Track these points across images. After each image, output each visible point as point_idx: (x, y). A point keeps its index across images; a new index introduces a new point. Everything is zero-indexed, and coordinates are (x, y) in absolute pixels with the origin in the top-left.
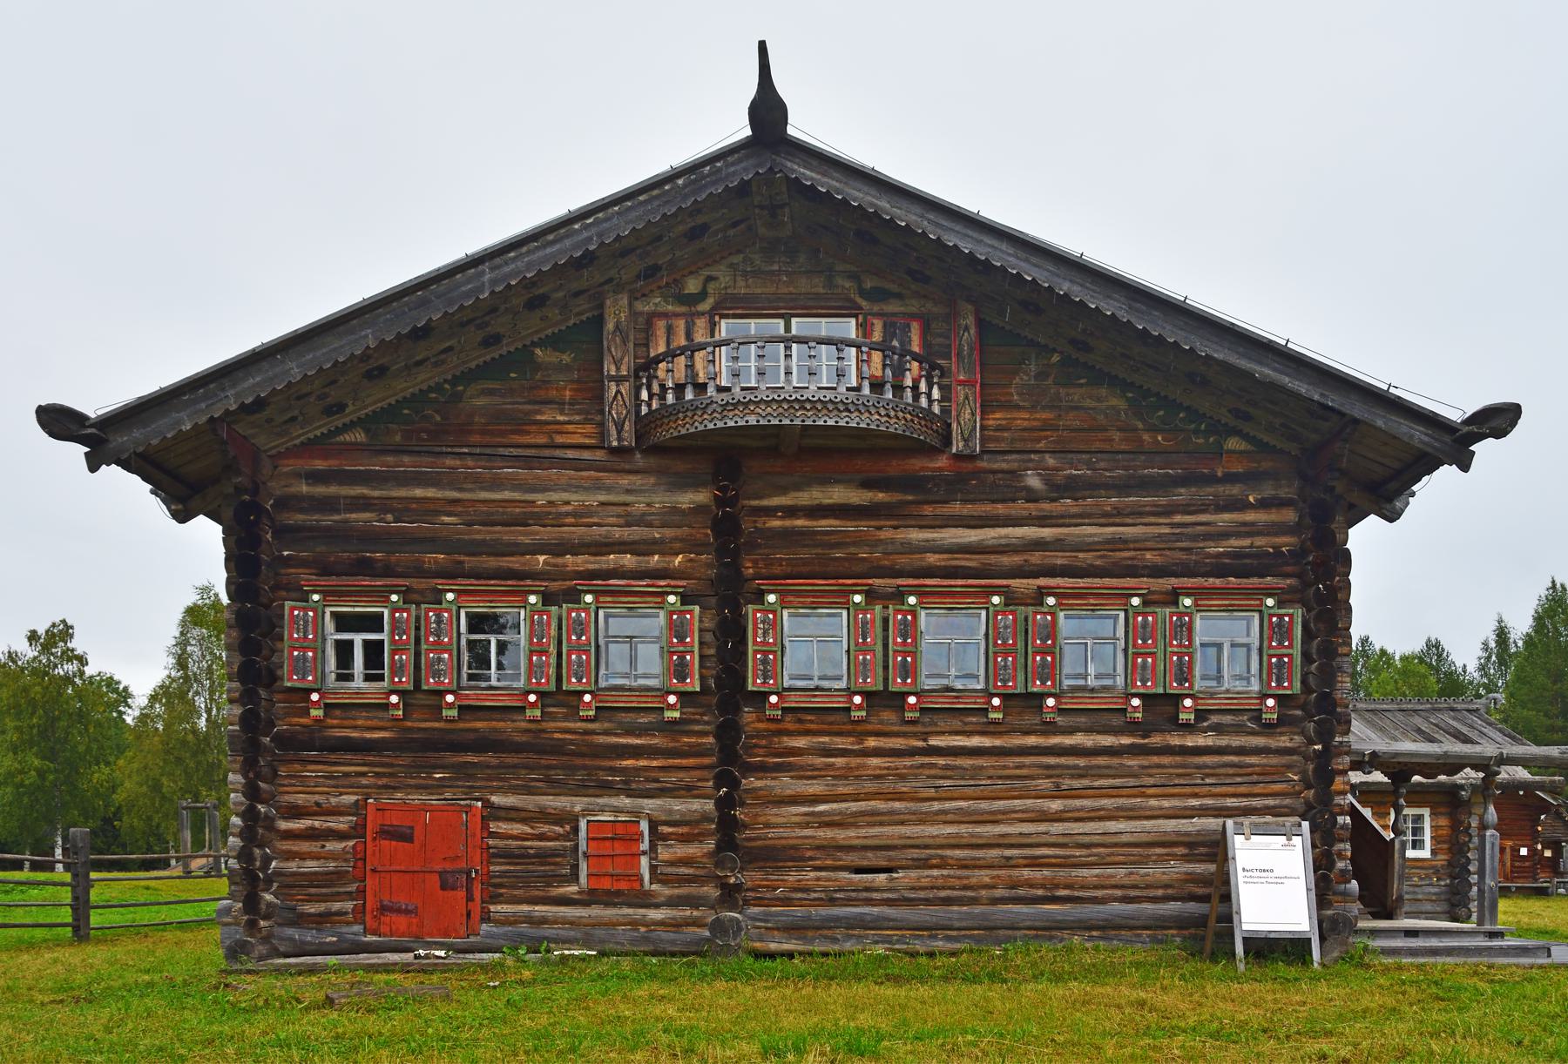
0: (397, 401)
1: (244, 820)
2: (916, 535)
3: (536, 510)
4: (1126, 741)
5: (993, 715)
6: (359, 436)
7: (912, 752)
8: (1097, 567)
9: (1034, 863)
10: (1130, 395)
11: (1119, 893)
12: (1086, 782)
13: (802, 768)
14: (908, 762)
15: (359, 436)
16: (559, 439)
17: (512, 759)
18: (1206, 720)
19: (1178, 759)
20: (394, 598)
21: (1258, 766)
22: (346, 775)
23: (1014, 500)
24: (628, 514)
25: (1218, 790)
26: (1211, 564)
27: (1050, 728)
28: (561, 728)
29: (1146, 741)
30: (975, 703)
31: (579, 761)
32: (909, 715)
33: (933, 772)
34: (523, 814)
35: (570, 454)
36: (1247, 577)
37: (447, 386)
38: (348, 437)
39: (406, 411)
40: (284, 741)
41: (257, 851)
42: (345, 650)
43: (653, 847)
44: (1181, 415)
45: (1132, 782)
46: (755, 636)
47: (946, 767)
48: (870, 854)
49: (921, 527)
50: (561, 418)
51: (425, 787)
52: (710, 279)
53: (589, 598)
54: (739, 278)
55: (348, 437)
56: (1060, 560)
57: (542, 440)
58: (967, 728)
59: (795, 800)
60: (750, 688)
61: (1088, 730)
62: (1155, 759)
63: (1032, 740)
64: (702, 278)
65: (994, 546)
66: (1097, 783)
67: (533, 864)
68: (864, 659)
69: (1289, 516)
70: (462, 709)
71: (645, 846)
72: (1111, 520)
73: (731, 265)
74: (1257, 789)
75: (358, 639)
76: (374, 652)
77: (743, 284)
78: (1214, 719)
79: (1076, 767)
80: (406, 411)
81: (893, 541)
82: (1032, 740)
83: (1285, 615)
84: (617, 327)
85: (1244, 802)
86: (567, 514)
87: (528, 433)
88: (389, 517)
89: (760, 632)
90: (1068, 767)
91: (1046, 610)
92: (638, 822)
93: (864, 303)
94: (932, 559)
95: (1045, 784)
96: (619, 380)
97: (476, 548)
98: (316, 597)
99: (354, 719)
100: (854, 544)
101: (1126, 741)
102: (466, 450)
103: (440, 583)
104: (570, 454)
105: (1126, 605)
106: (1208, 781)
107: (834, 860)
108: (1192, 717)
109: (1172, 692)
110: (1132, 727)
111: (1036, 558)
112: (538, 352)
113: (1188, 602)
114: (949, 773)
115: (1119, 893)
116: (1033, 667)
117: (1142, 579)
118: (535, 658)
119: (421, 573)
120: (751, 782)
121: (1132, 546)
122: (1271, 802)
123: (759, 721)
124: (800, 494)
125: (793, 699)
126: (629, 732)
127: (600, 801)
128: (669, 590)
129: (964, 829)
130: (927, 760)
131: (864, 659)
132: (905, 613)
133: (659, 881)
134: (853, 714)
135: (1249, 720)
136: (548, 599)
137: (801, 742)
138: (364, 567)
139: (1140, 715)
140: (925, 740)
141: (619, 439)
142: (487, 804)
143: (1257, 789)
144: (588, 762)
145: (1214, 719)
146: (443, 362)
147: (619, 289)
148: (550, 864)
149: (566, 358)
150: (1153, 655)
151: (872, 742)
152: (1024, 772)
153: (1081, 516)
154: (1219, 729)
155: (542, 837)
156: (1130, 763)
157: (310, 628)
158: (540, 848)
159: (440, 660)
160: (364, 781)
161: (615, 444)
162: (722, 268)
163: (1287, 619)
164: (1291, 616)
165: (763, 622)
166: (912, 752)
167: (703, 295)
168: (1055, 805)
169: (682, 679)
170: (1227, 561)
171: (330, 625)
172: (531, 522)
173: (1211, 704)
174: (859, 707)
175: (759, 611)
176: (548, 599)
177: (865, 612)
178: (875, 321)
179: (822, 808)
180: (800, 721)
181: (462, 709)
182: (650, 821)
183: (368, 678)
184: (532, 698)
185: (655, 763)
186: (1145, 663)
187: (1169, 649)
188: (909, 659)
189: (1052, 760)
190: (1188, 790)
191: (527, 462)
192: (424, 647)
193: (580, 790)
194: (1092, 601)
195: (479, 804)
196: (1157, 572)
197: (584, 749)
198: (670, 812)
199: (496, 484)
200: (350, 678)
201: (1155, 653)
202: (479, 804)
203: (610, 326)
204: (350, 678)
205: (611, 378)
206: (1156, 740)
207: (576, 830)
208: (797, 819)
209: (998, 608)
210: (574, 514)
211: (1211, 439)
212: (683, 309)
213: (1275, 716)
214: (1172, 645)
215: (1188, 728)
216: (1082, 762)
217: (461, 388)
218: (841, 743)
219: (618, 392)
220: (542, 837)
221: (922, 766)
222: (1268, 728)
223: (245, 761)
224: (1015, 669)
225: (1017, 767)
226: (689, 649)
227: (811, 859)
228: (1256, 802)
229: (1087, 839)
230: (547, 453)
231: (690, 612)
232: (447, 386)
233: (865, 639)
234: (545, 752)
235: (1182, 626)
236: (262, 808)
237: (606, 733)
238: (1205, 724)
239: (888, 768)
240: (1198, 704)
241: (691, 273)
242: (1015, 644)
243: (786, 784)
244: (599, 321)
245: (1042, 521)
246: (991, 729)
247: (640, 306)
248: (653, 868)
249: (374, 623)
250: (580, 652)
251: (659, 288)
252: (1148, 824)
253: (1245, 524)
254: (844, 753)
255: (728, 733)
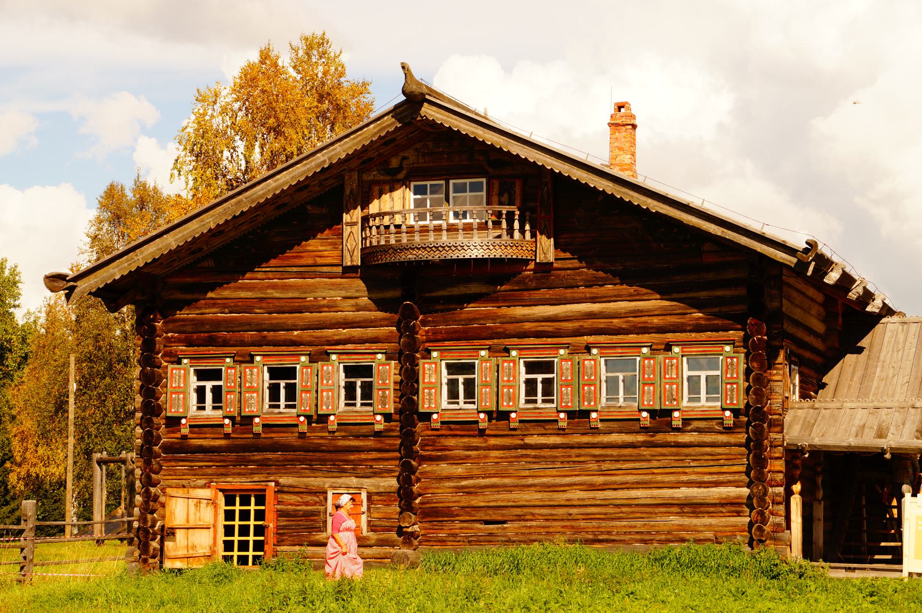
0: (231, 241)
1: (143, 497)
2: (519, 311)
3: (307, 304)
4: (641, 438)
5: (561, 424)
6: (210, 263)
7: (516, 447)
8: (623, 329)
9: (588, 518)
10: (645, 219)
11: (638, 537)
12: (619, 466)
13: (453, 458)
14: (513, 453)
15: (210, 263)
16: (320, 261)
17: (290, 455)
18: (690, 425)
19: (674, 450)
20: (228, 360)
21: (724, 454)
22: (200, 467)
23: (578, 287)
24: (357, 305)
25: (699, 470)
26: (693, 325)
27: (595, 431)
28: (317, 437)
29: (653, 439)
30: (551, 416)
31: (328, 456)
32: (512, 425)
33: (528, 460)
34: (297, 490)
35: (325, 269)
36: (717, 331)
37: (259, 231)
38: (205, 264)
39: (236, 247)
40: (167, 448)
41: (149, 517)
42: (201, 391)
43: (369, 509)
44: (675, 231)
45: (645, 465)
46: (424, 379)
47: (535, 457)
48: (490, 512)
49: (523, 306)
50: (321, 248)
51: (244, 475)
52: (404, 158)
53: (334, 357)
54: (420, 157)
55: (205, 264)
56: (601, 323)
57: (310, 262)
58: (547, 432)
59: (449, 478)
60: (421, 410)
61: (620, 432)
62: (659, 450)
63: (586, 439)
64: (400, 158)
65: (564, 317)
66: (624, 466)
67: (301, 520)
68: (486, 391)
69: (742, 291)
70: (264, 426)
71: (364, 508)
72: (634, 298)
73: (416, 150)
74: (725, 469)
75: (209, 385)
76: (217, 393)
77: (423, 161)
78: (695, 424)
79: (612, 456)
80: (236, 247)
81: (504, 316)
82: (586, 439)
83: (734, 357)
84: (351, 192)
85: (715, 478)
86: (324, 306)
87: (302, 257)
88: (227, 310)
89: (427, 376)
90: (607, 456)
91: (590, 358)
92: (360, 493)
93: (490, 170)
94: (528, 326)
95: (594, 466)
96: (353, 224)
97: (275, 328)
98: (185, 361)
99: (205, 434)
100: (483, 319)
101: (641, 438)
102: (268, 269)
103: (252, 350)
104: (325, 269)
105: (639, 352)
106: (692, 464)
107: (470, 516)
108: (680, 423)
109: (665, 408)
110: (645, 430)
111: (588, 324)
112: (309, 207)
113: (676, 349)
114: (537, 460)
115: (638, 537)
116: (583, 394)
117: (651, 335)
118: (303, 395)
119: (243, 344)
120: (425, 467)
121: (646, 314)
122: (730, 478)
123: (428, 429)
124: (453, 289)
125: (447, 416)
126: (357, 437)
127: (340, 481)
128: (377, 351)
129: (545, 496)
130: (524, 452)
131: (486, 391)
132: (510, 362)
133: (372, 531)
134: (480, 424)
135: (716, 425)
136: (313, 359)
137: (451, 442)
138: (211, 342)
139: (648, 423)
140: (522, 440)
141: (352, 261)
142: (277, 484)
143: (725, 469)
144: (333, 456)
145: (695, 424)
146: (255, 220)
147: (351, 170)
148: (312, 520)
149: (324, 211)
150: (653, 384)
151: (493, 441)
152: (582, 459)
153: (616, 296)
154: (699, 431)
155: (307, 504)
156: (645, 453)
157: (182, 380)
158: (306, 511)
159: (252, 397)
160: (209, 471)
161: (349, 264)
162: (411, 151)
163: (735, 360)
164: (737, 357)
165: (429, 369)
166: (516, 447)
167: (400, 169)
168: (600, 479)
169: (384, 404)
170: (703, 322)
171: (193, 378)
172: (304, 311)
173: (692, 415)
174: (483, 420)
175: (427, 363)
176: (313, 359)
177: (486, 361)
178: (494, 181)
179: (464, 483)
180: (451, 430)
181: (264, 426)
182: (368, 493)
183: (214, 408)
184: (302, 419)
185: (370, 457)
186: (649, 390)
187: (663, 380)
188: (511, 390)
189: (597, 452)
190: (680, 470)
191: (301, 275)
192: (243, 389)
193: (329, 473)
194: (619, 351)
195: (273, 484)
196: (661, 330)
197: (331, 449)
198: (378, 487)
199: (285, 288)
200: (203, 408)
201: (654, 384)
202: (273, 484)
203: (348, 192)
204: (203, 408)
205: (348, 224)
206: (660, 437)
207: (326, 499)
208: (448, 490)
209: (563, 357)
210: (328, 307)
211: (694, 245)
212: (388, 178)
213: (732, 422)
214: (665, 378)
215: (678, 430)
216: (615, 452)
217: (266, 232)
218: (475, 442)
219: (351, 232)
220: (307, 504)
221: (522, 456)
222: (728, 430)
223: (145, 462)
224: (572, 396)
225: (577, 456)
226: (387, 387)
227: (457, 515)
228: (722, 478)
229: (618, 502)
230: (313, 269)
231: (388, 364)
232: (259, 231)
233: (486, 378)
234: (310, 451)
235: (672, 365)
236: (152, 490)
237: (344, 438)
238: (689, 428)
239: (502, 458)
240: (683, 415)
241: (393, 156)
242: (572, 379)
243: (444, 468)
244: (341, 188)
245: (593, 300)
246: (561, 432)
247: (365, 177)
248: (369, 522)
249: (215, 375)
250: (328, 391)
251: (376, 165)
252: (656, 492)
253: (717, 297)
254: (477, 448)
255: (408, 438)
